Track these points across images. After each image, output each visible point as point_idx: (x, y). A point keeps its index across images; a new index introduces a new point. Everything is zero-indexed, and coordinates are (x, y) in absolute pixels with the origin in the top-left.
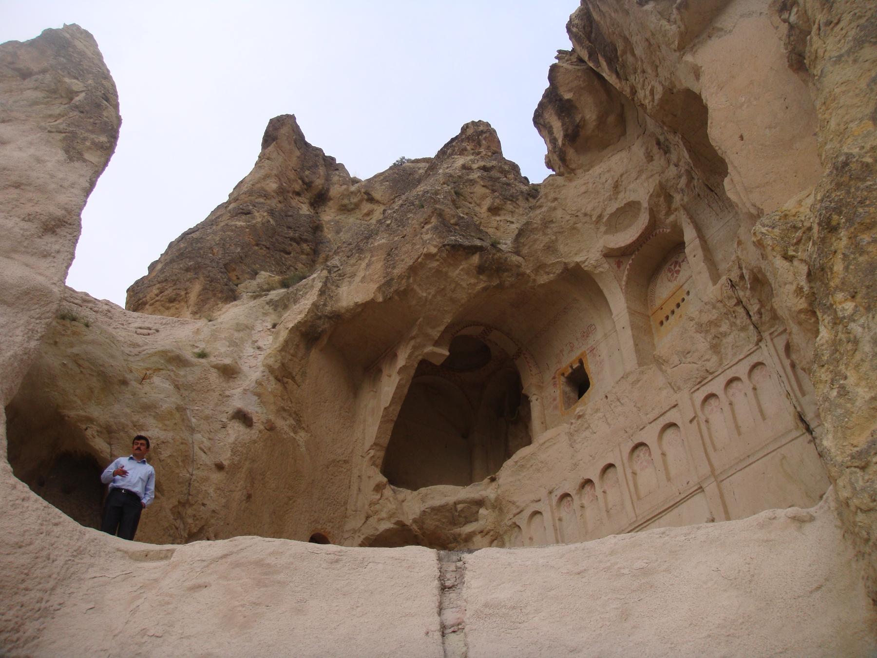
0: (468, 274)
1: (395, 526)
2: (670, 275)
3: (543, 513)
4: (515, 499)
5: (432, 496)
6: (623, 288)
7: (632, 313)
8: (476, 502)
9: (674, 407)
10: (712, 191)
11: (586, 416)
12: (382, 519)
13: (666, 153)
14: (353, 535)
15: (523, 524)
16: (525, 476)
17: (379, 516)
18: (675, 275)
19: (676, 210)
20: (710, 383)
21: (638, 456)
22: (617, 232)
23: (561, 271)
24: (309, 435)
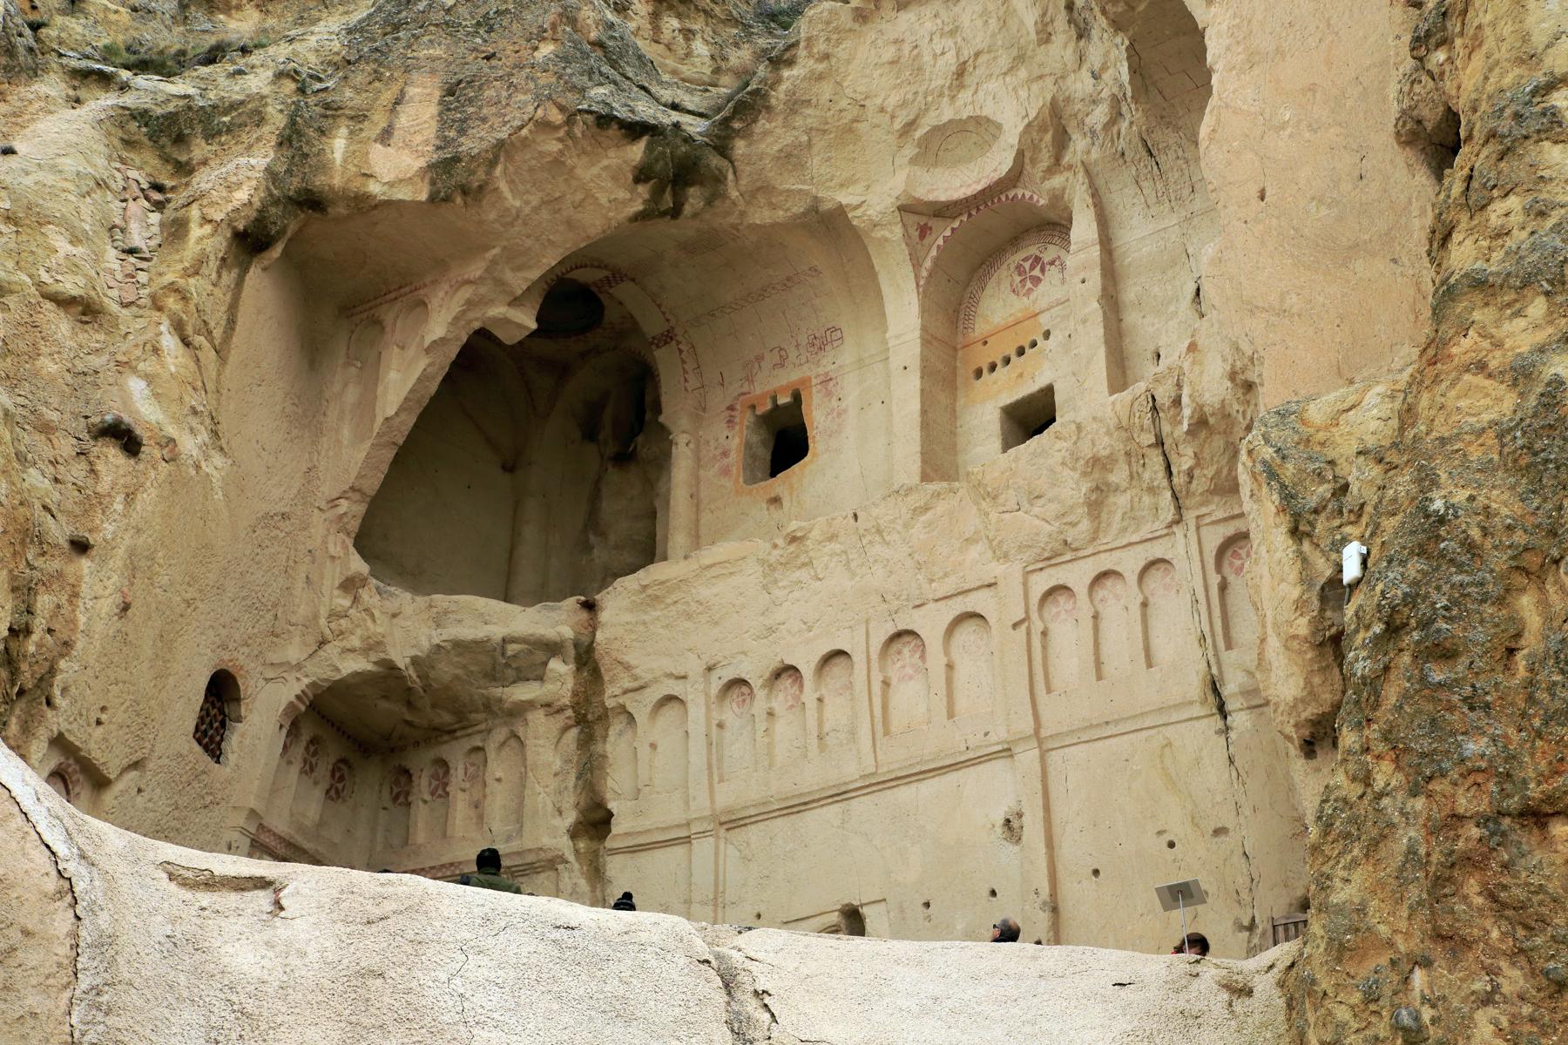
0: (615, 179)
1: (380, 669)
2: (1018, 279)
3: (689, 705)
4: (630, 658)
5: (458, 617)
6: (922, 283)
7: (928, 339)
8: (547, 645)
9: (989, 586)
10: (1151, 155)
11: (809, 543)
12: (352, 651)
13: (1080, 37)
14: (284, 674)
15: (641, 716)
16: (658, 619)
17: (345, 643)
18: (1029, 285)
19: (1070, 167)
20: (1064, 566)
21: (899, 653)
22: (935, 165)
23: (802, 210)
24: (230, 462)
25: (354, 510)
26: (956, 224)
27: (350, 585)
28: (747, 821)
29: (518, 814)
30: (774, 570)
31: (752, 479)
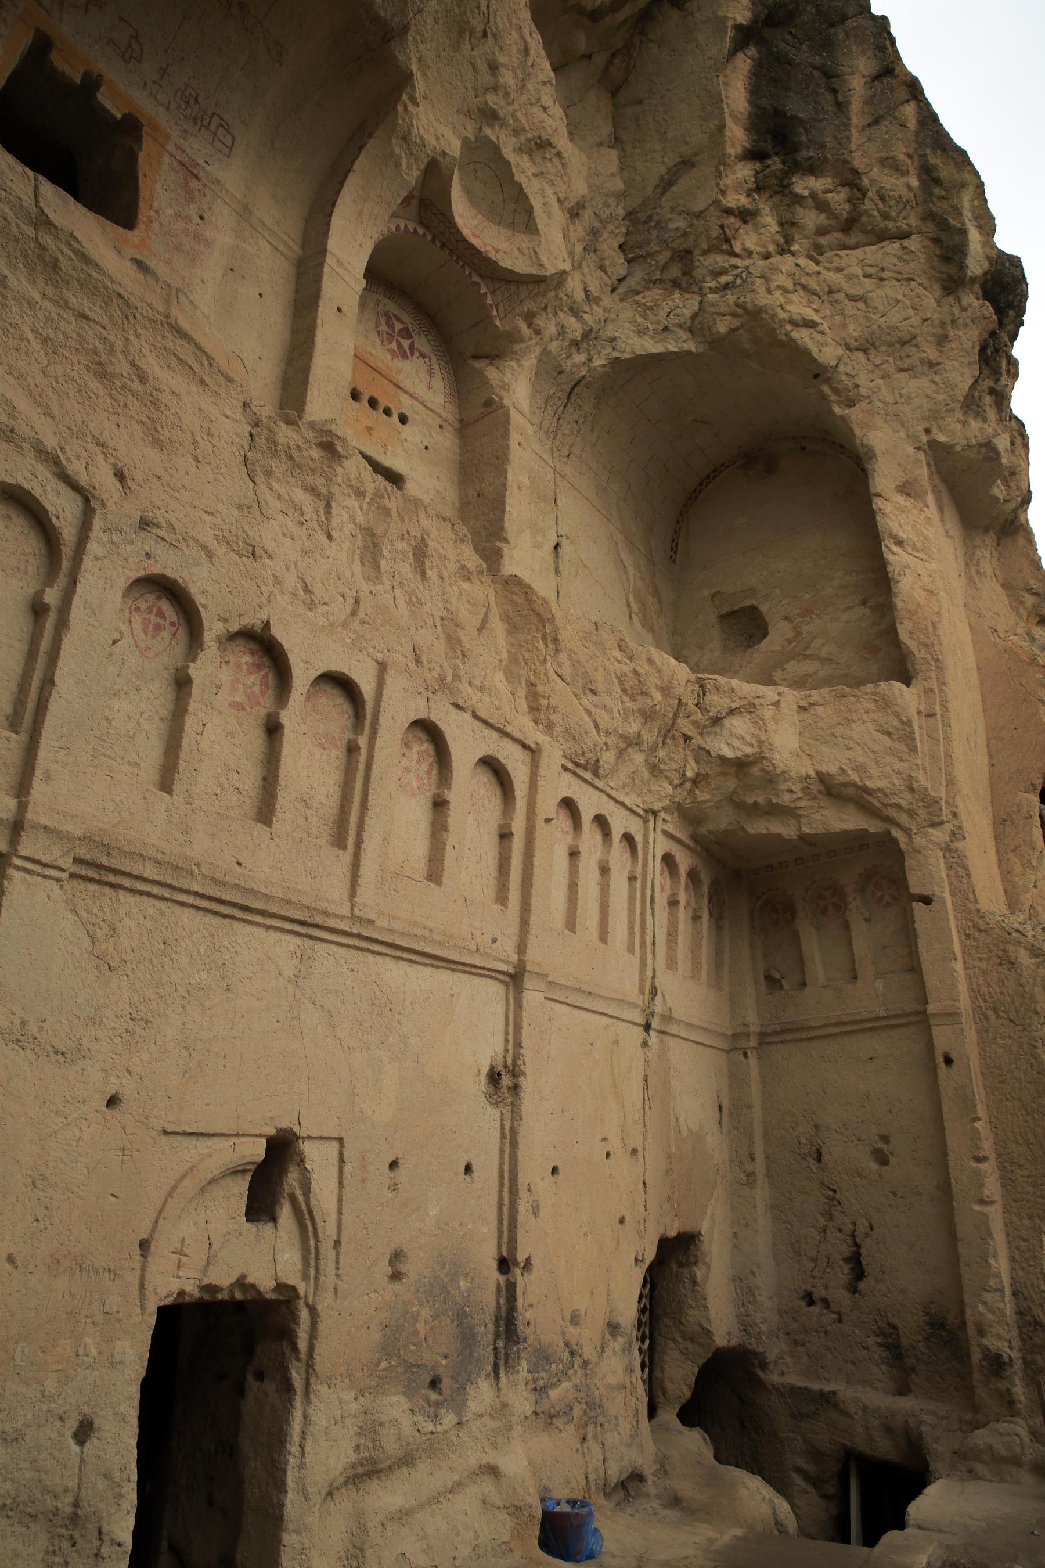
11: (339, 470)
16: (31, 303)
26: (421, 231)
28: (127, 882)
30: (275, 453)
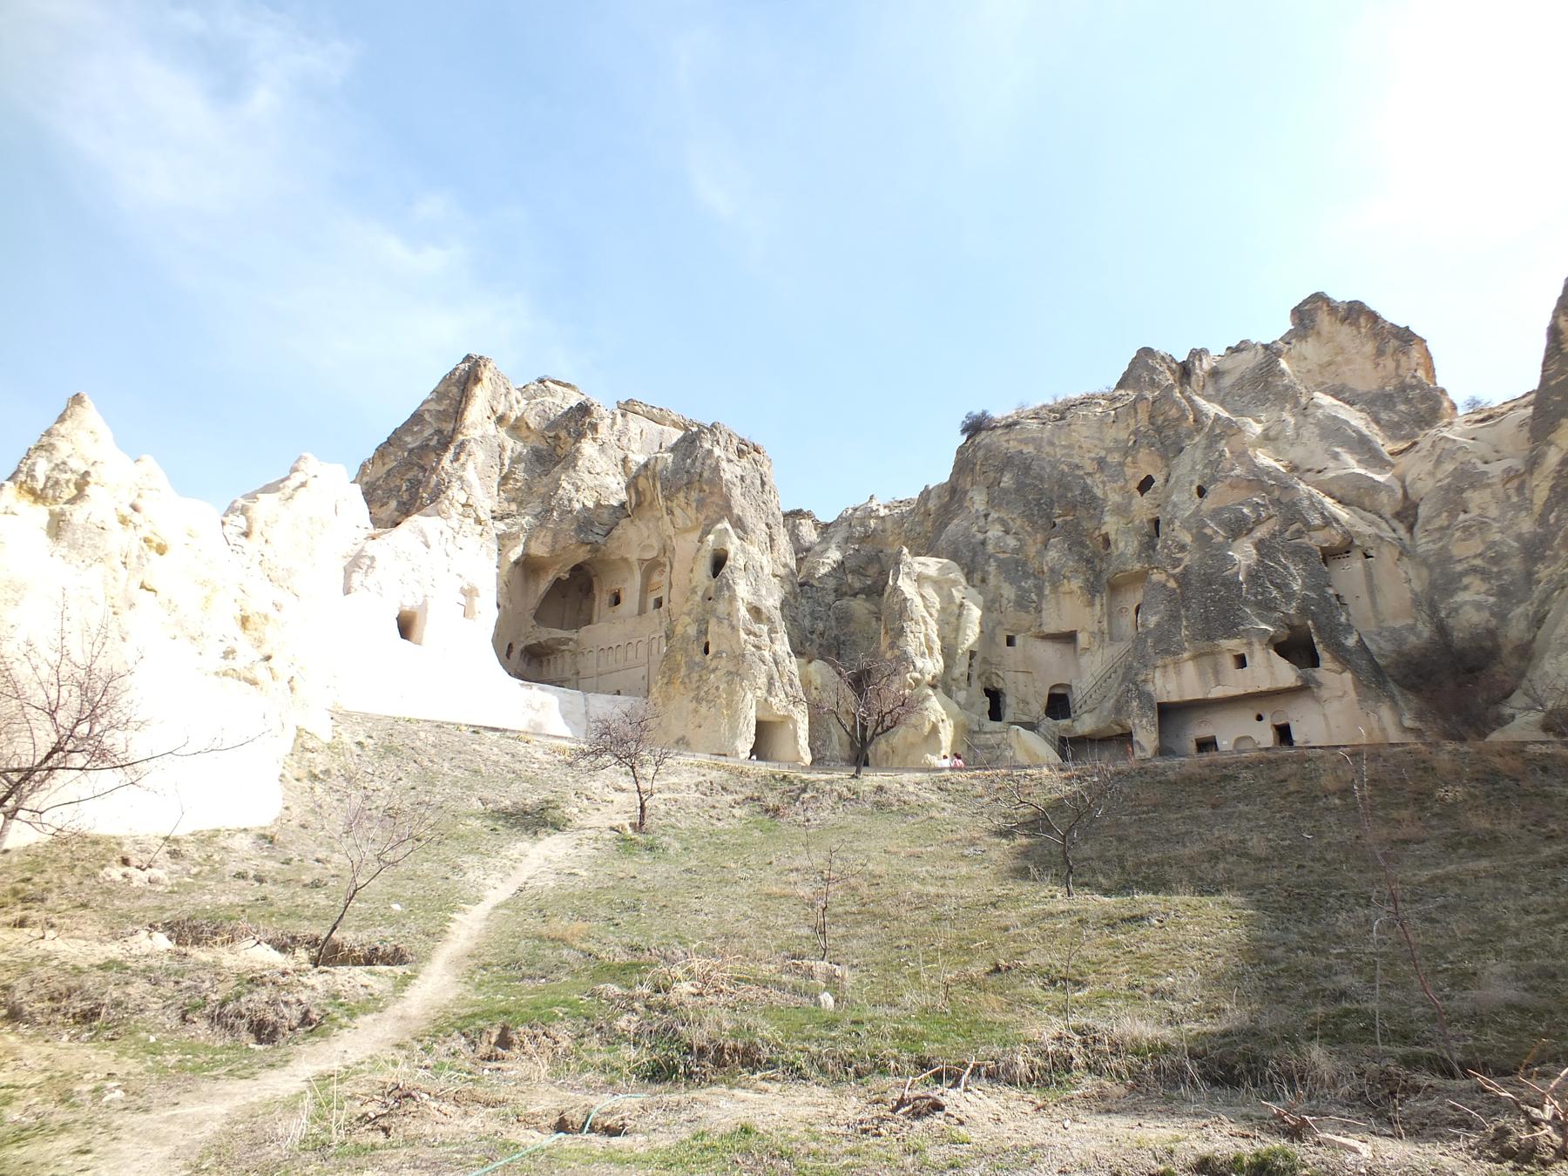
25: (533, 611)
27: (533, 626)
29: (563, 671)
31: (610, 607)
